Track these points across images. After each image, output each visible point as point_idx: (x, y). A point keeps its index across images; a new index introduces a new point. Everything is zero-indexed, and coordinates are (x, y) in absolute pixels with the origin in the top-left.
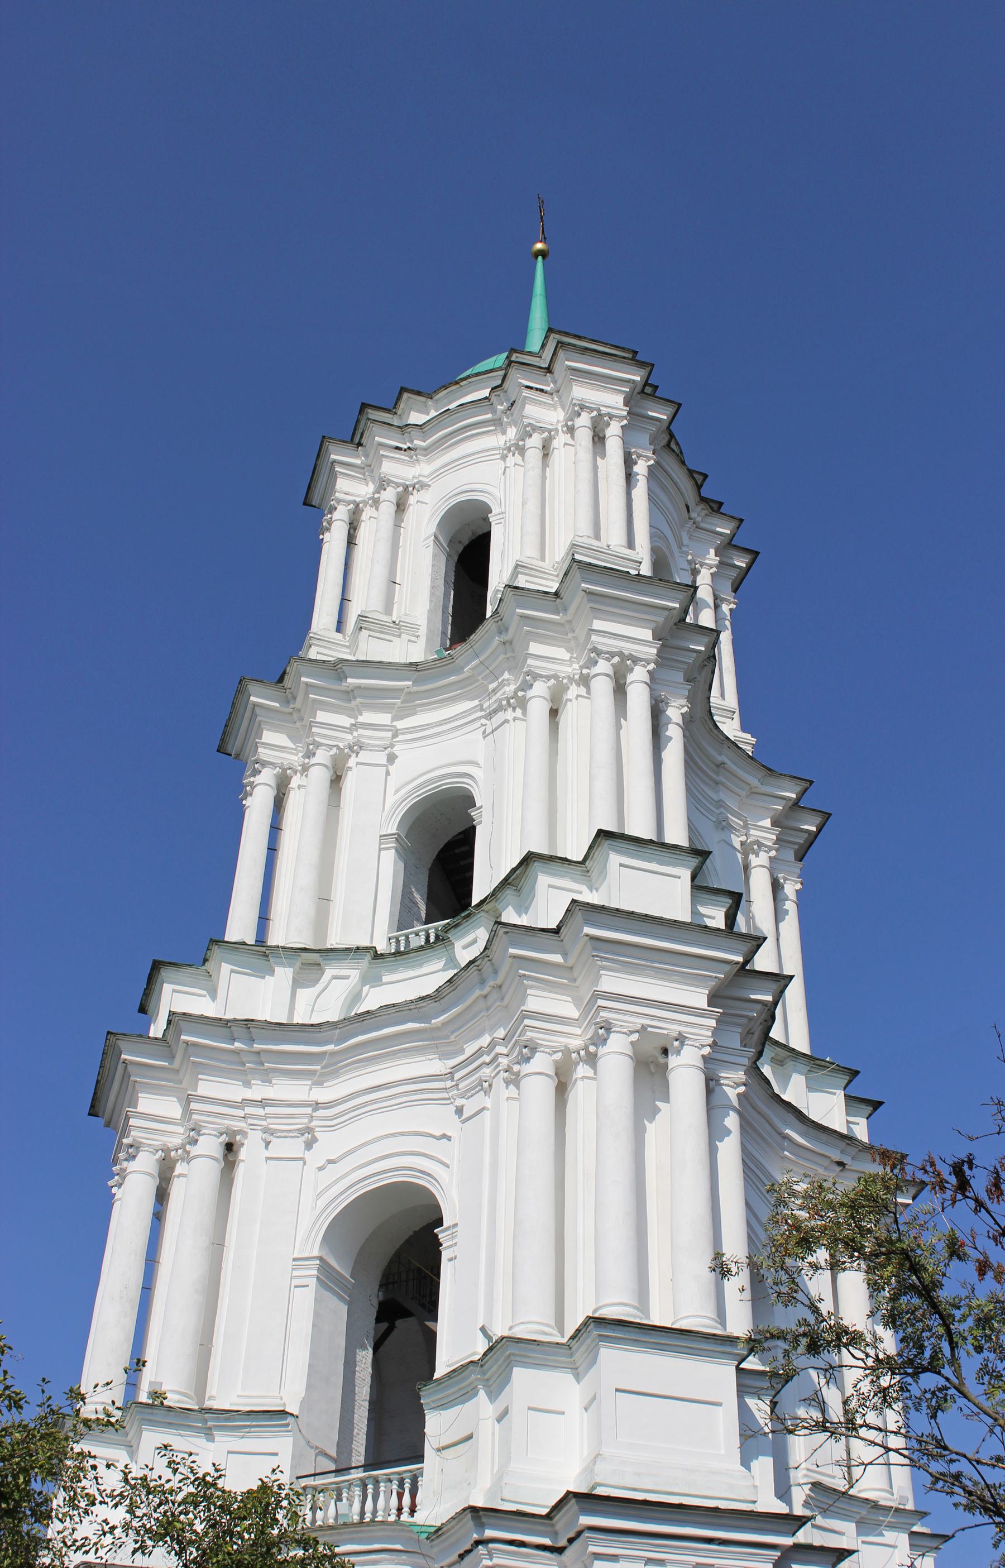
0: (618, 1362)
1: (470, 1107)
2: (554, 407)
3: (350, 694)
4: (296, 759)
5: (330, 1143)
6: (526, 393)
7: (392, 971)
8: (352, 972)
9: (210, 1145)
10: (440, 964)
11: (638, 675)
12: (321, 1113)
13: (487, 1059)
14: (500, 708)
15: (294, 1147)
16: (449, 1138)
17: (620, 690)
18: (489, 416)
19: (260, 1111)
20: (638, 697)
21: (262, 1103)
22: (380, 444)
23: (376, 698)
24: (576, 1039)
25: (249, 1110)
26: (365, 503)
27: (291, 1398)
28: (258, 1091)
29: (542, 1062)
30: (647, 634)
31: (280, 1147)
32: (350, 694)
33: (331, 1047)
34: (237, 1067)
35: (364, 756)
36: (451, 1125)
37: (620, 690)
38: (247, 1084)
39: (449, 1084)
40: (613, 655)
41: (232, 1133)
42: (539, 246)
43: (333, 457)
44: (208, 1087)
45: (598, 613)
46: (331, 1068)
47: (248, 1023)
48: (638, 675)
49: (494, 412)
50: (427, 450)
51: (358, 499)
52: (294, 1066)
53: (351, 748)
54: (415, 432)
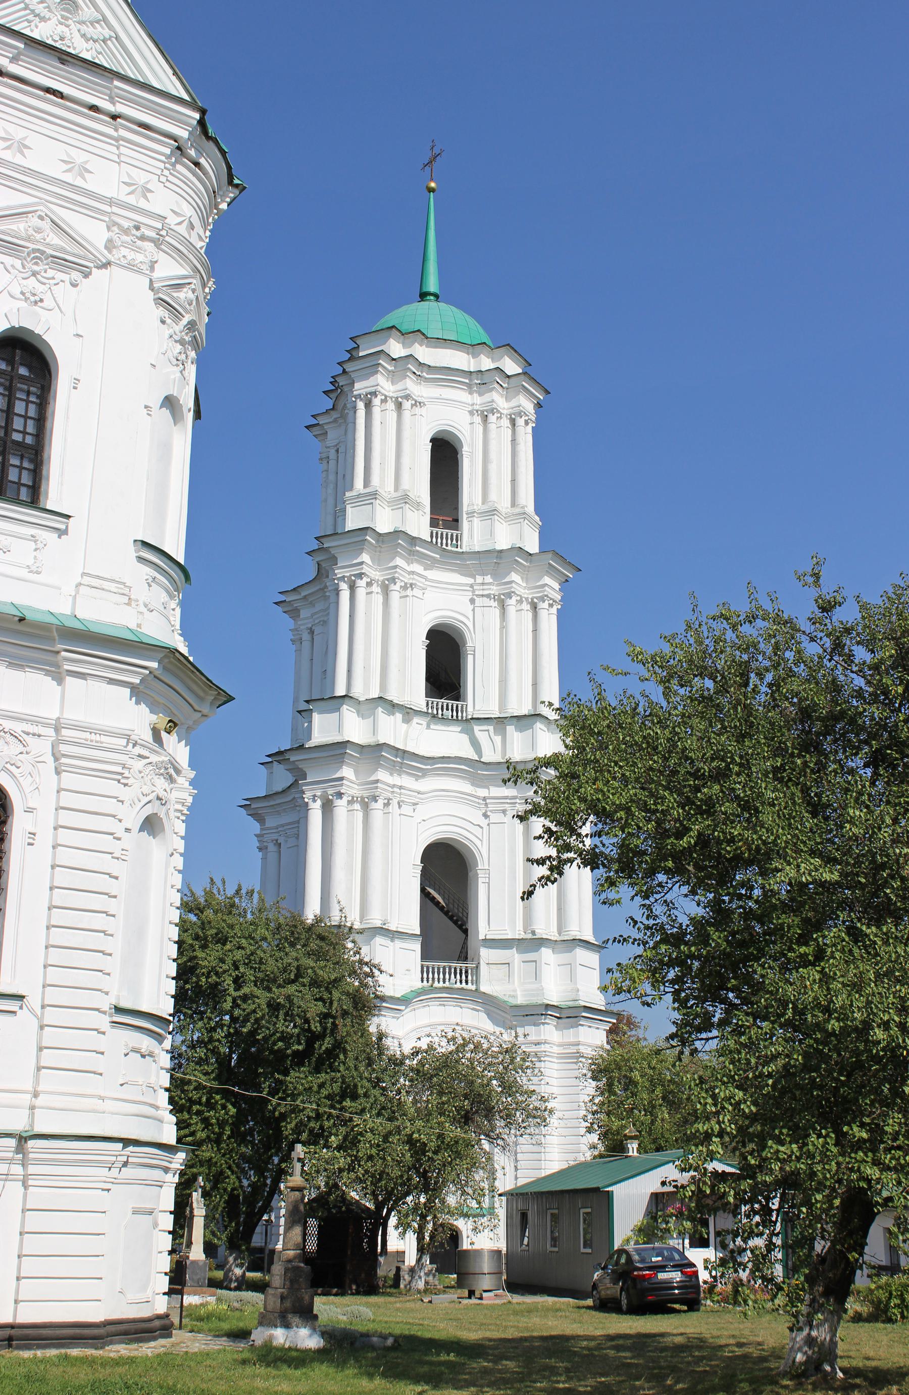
1: (494, 817)
2: (502, 396)
3: (412, 553)
5: (423, 811)
6: (496, 385)
7: (436, 724)
8: (423, 721)
10: (459, 729)
12: (420, 796)
13: (508, 801)
14: (488, 596)
16: (482, 828)
18: (467, 381)
19: (398, 790)
21: (401, 787)
22: (409, 369)
25: (396, 790)
26: (391, 398)
28: (396, 780)
30: (557, 586)
31: (406, 809)
33: (429, 767)
35: (417, 592)
36: (484, 822)
38: (391, 774)
39: (481, 802)
40: (551, 599)
41: (389, 800)
42: (433, 185)
43: (381, 361)
44: (382, 775)
46: (425, 773)
47: (404, 752)
49: (470, 380)
50: (427, 380)
51: (387, 394)
53: (411, 585)
54: (425, 369)
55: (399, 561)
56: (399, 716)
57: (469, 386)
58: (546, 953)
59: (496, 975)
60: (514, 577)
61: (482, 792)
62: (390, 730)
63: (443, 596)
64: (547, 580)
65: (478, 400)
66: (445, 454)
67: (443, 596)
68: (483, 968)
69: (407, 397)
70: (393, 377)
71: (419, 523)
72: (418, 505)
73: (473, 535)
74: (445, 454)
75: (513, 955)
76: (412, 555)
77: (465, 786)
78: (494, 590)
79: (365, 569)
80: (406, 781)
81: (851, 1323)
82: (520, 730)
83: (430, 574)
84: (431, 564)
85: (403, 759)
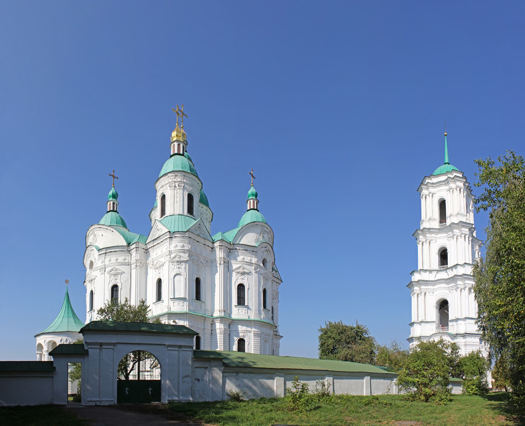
0: (468, 321)
1: (451, 291)
3: (431, 232)
4: (424, 240)
5: (435, 293)
8: (435, 272)
9: (423, 294)
11: (467, 236)
15: (431, 294)
17: (465, 237)
20: (467, 239)
23: (433, 233)
24: (463, 287)
27: (434, 320)
28: (427, 287)
29: (459, 289)
30: (468, 230)
32: (431, 232)
34: (425, 285)
36: (449, 293)
37: (465, 237)
44: (423, 287)
45: (462, 227)
46: (435, 285)
48: (467, 236)
52: (431, 285)
55: (427, 235)
56: (428, 272)
57: (445, 184)
58: (459, 322)
59: (453, 328)
60: (455, 230)
61: (449, 286)
62: (425, 276)
63: (441, 240)
64: (463, 229)
65: (447, 187)
66: (442, 204)
67: (441, 240)
68: (449, 327)
69: (430, 193)
70: (427, 189)
71: (436, 224)
72: (434, 219)
73: (448, 222)
74: (442, 204)
75: (454, 323)
76: (431, 233)
77: (445, 285)
78: (452, 235)
79: (420, 240)
80: (430, 287)
81: (477, 398)
82: (456, 269)
83: (437, 236)
84: (437, 233)
85: (426, 282)
